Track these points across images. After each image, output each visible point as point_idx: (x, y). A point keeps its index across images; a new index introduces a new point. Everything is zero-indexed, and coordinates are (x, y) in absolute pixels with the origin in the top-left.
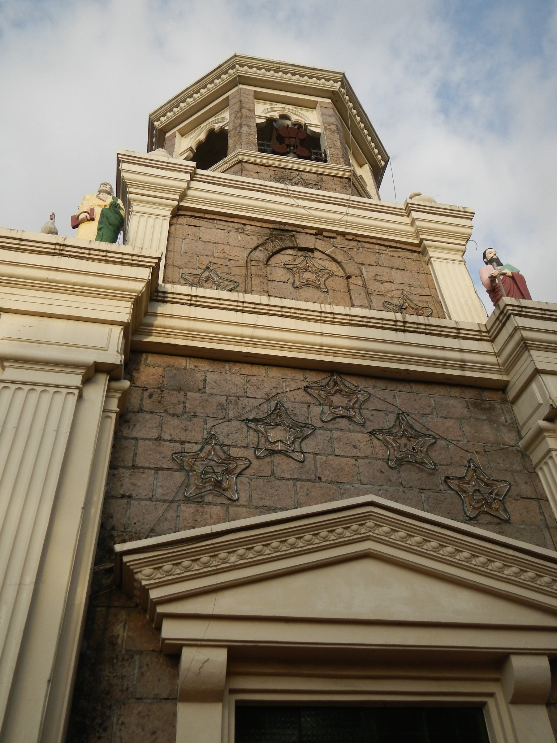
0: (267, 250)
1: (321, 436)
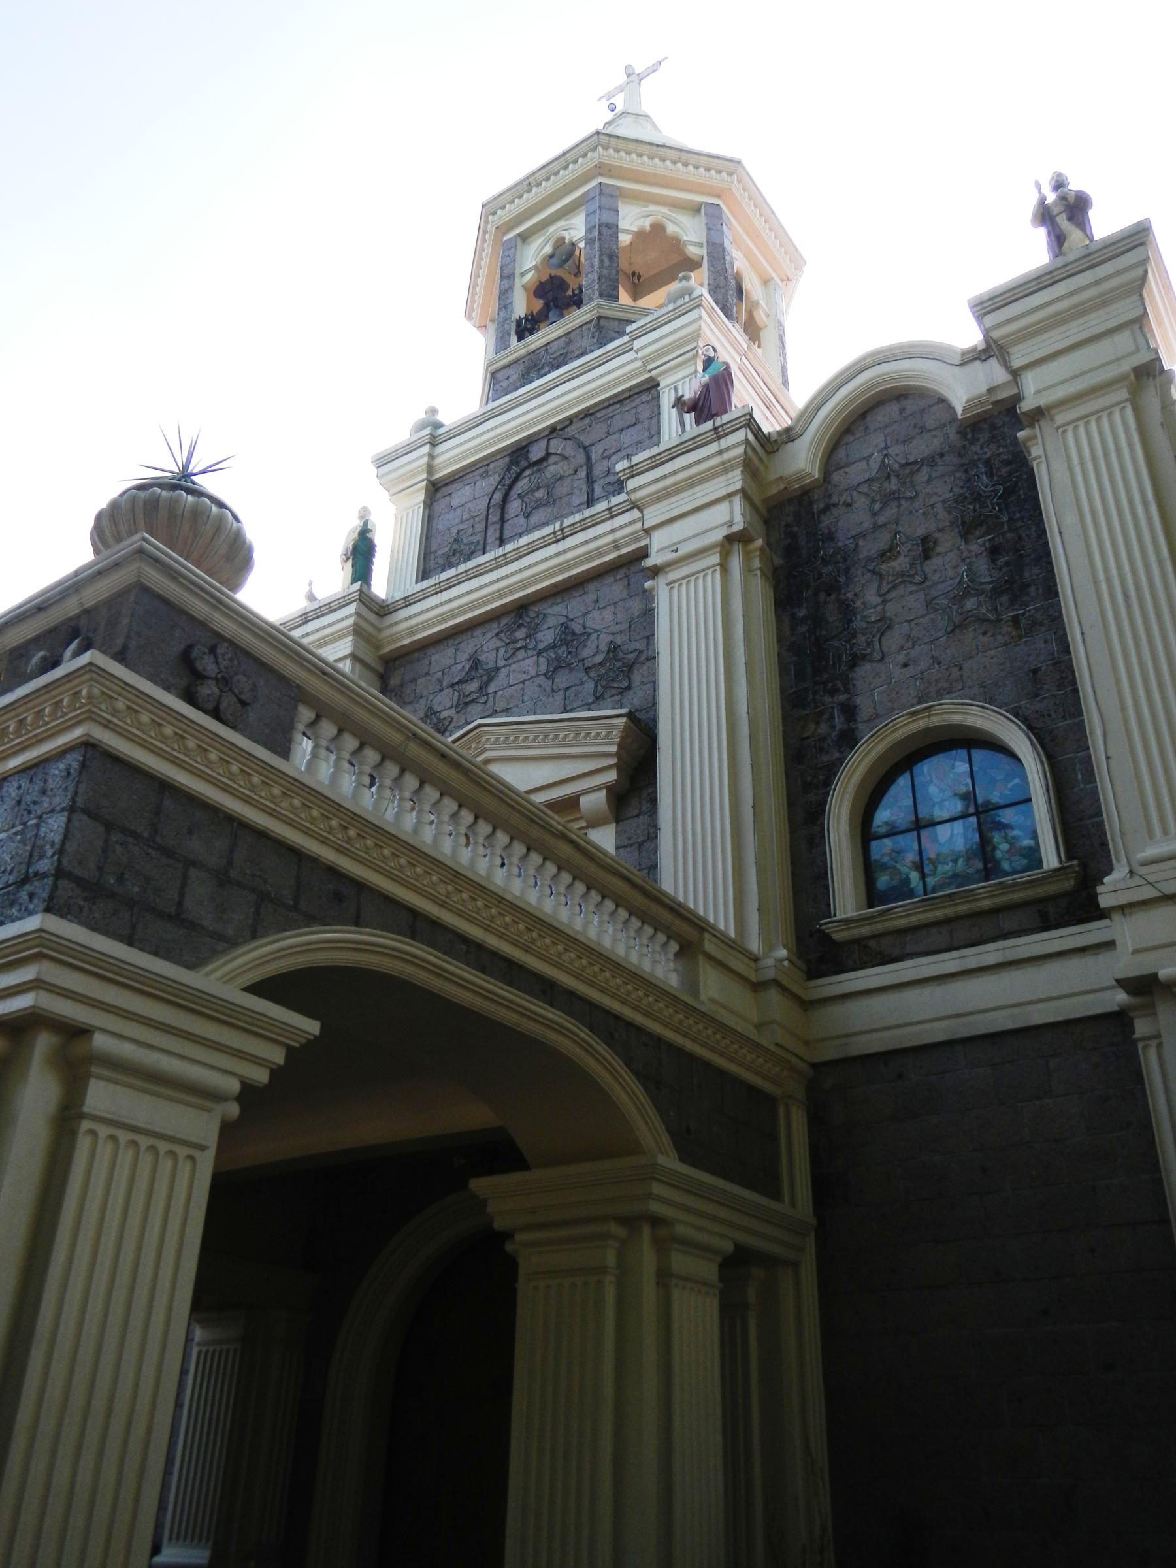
0: (504, 485)
1: (504, 671)
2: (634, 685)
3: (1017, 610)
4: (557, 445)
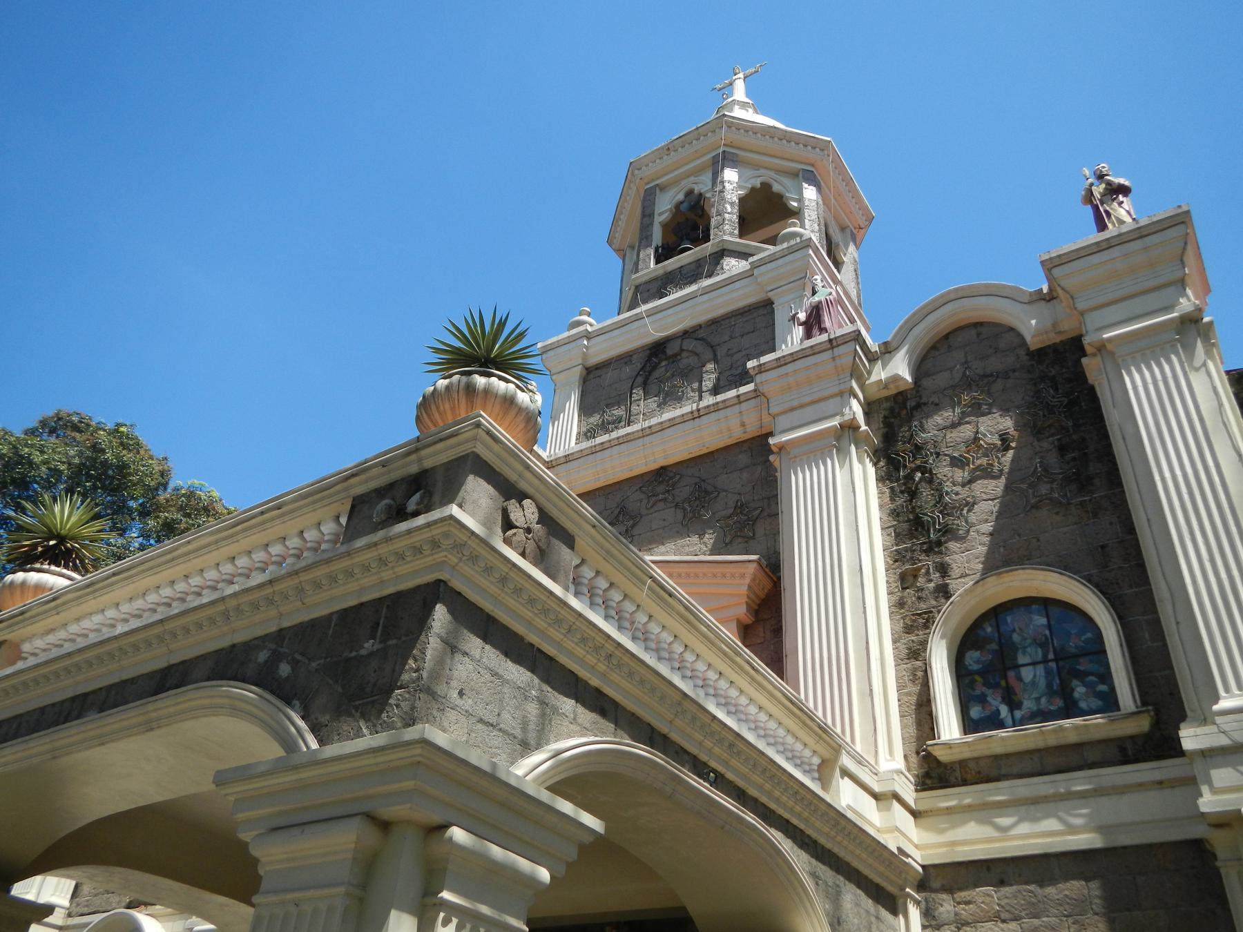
2: (757, 536)
3: (1084, 496)
4: (689, 344)
